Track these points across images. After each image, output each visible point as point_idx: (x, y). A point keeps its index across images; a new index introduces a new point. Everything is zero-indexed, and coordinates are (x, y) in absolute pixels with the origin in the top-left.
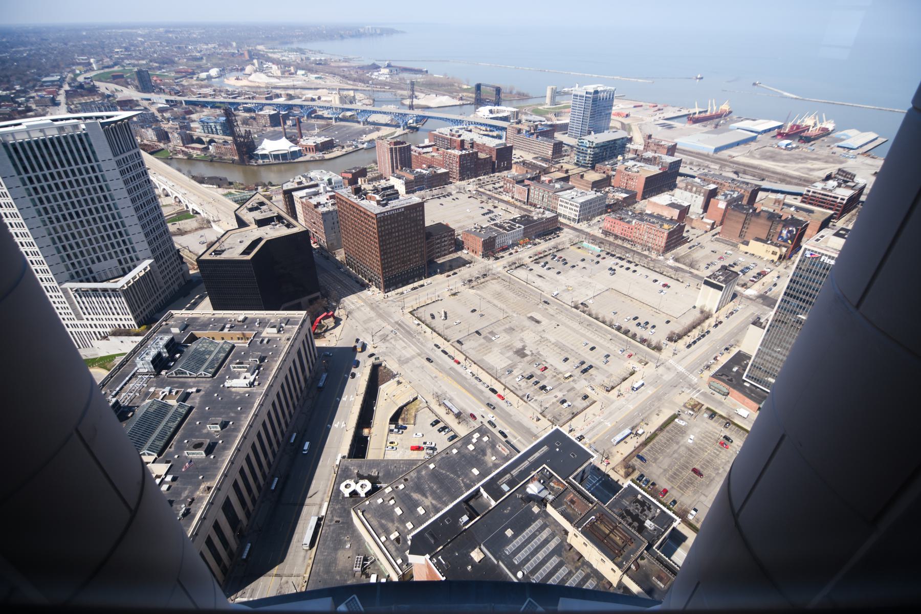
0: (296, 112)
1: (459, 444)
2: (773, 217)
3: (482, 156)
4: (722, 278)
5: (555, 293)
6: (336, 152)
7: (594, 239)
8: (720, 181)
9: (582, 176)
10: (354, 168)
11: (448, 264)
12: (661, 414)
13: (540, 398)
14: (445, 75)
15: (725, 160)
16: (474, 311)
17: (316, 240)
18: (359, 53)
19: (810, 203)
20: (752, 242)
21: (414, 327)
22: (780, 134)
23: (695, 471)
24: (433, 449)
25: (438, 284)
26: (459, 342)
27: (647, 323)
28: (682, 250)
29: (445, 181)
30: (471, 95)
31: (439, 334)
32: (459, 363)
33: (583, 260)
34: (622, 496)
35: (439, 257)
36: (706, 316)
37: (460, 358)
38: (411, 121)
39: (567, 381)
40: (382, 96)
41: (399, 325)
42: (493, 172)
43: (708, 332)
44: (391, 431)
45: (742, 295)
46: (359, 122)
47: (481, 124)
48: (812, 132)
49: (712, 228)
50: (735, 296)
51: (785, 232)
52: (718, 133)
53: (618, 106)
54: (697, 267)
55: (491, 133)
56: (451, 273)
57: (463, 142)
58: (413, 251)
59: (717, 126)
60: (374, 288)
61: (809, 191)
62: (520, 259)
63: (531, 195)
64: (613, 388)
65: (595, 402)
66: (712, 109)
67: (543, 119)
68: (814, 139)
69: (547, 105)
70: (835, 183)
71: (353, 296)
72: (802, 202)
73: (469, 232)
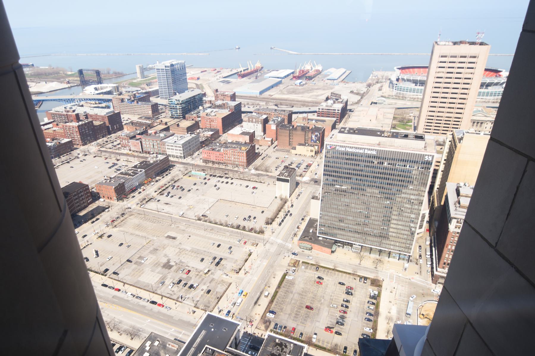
4: (286, 174)
5: (181, 213)
8: (268, 112)
9: (178, 125)
12: (276, 277)
13: (190, 296)
14: (50, 66)
15: (268, 99)
16: (121, 244)
22: (294, 77)
23: (308, 307)
26: (115, 273)
27: (250, 217)
28: (258, 162)
30: (76, 79)
32: (119, 290)
33: (195, 184)
34: (266, 346)
35: (80, 210)
36: (285, 201)
37: (119, 285)
39: (207, 275)
42: (110, 134)
45: (301, 182)
47: (90, 100)
48: (311, 73)
49: (272, 143)
50: (297, 184)
51: (313, 137)
52: (259, 82)
53: (190, 73)
54: (270, 171)
55: (100, 105)
56: (94, 219)
59: (256, 78)
62: (147, 195)
63: (144, 145)
64: (240, 269)
65: (231, 284)
66: (251, 67)
67: (139, 89)
68: (314, 77)
69: (139, 79)
70: (332, 102)
73: (101, 184)
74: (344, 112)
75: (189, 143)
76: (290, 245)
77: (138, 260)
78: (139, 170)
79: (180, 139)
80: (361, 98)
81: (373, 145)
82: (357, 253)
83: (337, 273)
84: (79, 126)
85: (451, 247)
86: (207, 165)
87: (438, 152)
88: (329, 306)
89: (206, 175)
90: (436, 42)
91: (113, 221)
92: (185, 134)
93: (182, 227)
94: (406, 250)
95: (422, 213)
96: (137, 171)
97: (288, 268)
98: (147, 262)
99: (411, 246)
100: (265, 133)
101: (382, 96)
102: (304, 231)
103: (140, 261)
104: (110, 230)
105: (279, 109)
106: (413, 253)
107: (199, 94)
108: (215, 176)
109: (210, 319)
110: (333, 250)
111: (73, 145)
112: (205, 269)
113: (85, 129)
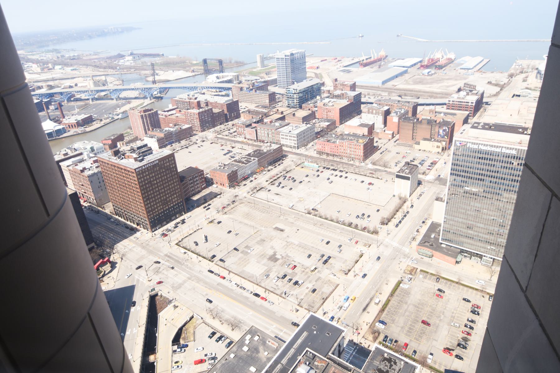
0: (57, 98)
1: (235, 349)
2: (430, 122)
4: (407, 171)
5: (291, 205)
6: (96, 125)
8: (390, 103)
9: (294, 115)
10: (113, 135)
11: (203, 199)
12: (389, 283)
16: (230, 232)
17: (85, 199)
18: (106, 47)
19: (452, 109)
21: (182, 256)
22: (422, 66)
23: (424, 322)
24: (214, 358)
25: (196, 217)
27: (363, 215)
28: (376, 156)
29: (190, 134)
31: (204, 258)
33: (307, 176)
38: (156, 93)
39: (314, 273)
40: (129, 77)
41: (169, 257)
42: (227, 121)
43: (408, 212)
44: (175, 351)
45: (424, 180)
46: (112, 99)
47: (211, 88)
48: (442, 62)
49: (393, 137)
51: (441, 131)
53: (310, 62)
54: (389, 166)
55: (220, 93)
58: (171, 194)
59: (380, 67)
60: (142, 230)
64: (349, 271)
65: (338, 285)
66: (374, 56)
67: (258, 78)
68: (444, 66)
69: (259, 68)
71: (126, 240)
74: (479, 105)
75: (304, 133)
76: (406, 250)
77: (244, 249)
78: (252, 158)
79: (294, 128)
80: (501, 90)
81: (514, 143)
82: (487, 266)
83: (461, 287)
84: (199, 113)
86: (321, 157)
88: (449, 324)
89: (319, 167)
91: (224, 208)
92: (300, 124)
93: (291, 220)
96: (250, 159)
97: (404, 275)
98: (253, 253)
101: (527, 88)
102: (425, 236)
103: (247, 250)
104: (220, 217)
105: (403, 100)
108: (329, 169)
109: (313, 320)
110: (458, 260)
111: (192, 131)
112: (312, 266)
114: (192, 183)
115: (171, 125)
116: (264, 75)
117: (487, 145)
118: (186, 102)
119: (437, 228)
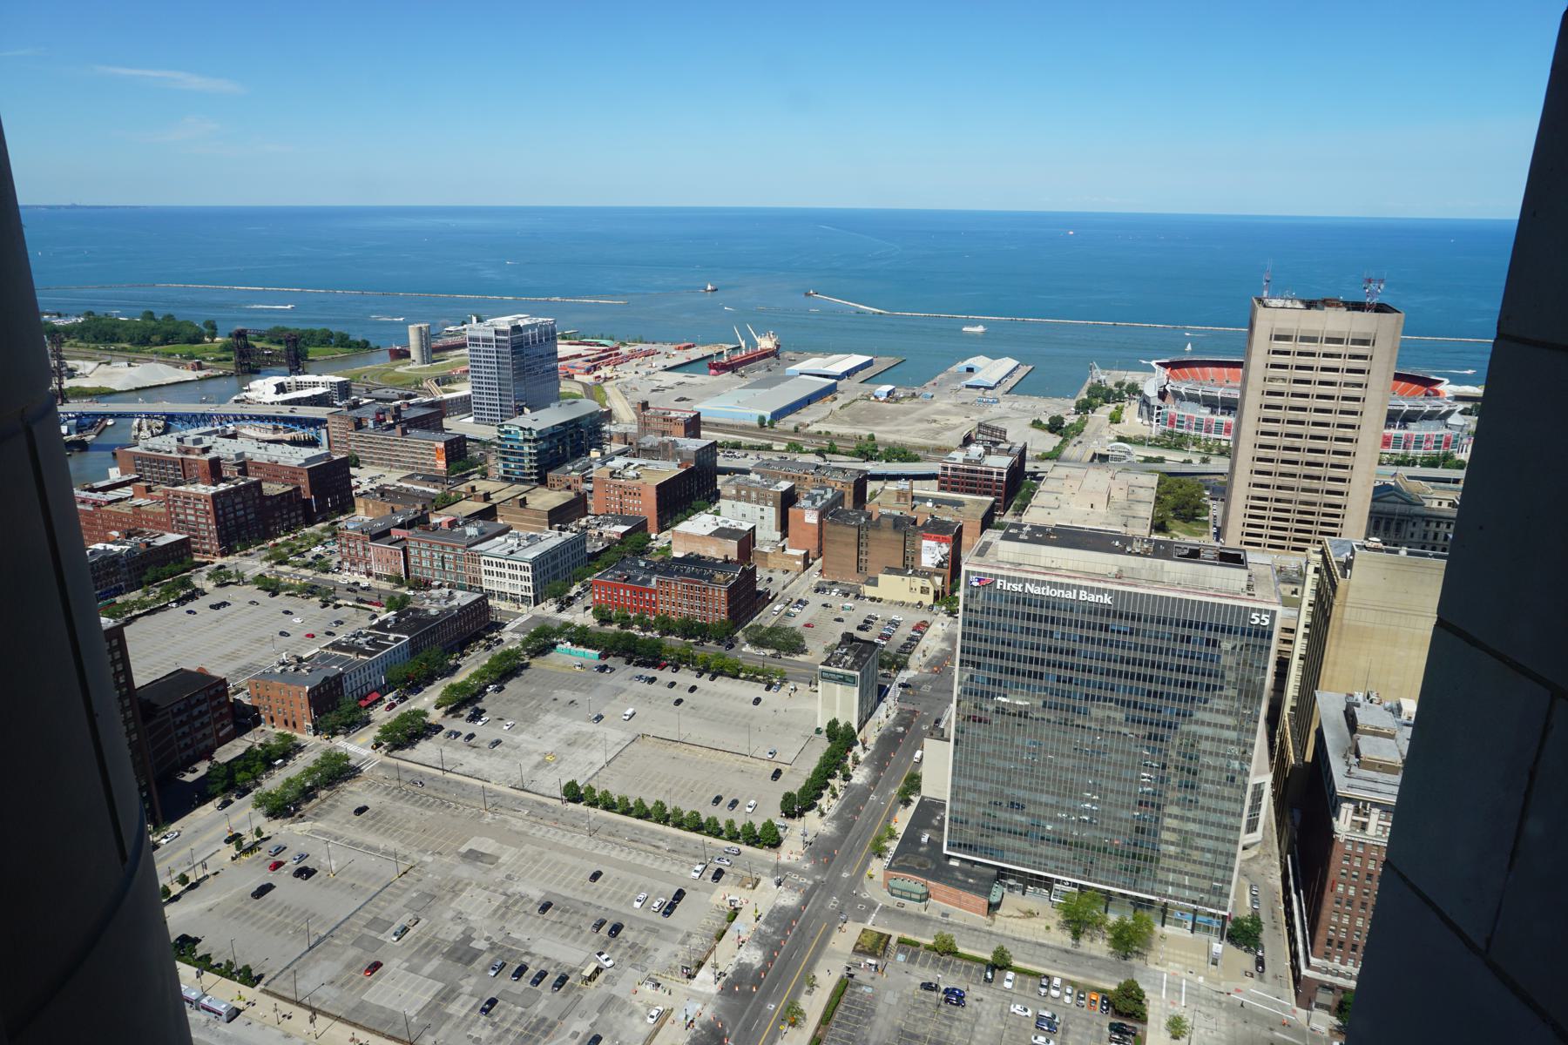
2: (899, 523)
3: (272, 489)
7: (581, 637)
8: (794, 472)
9: (523, 502)
20: (882, 578)
39: (593, 984)
49: (807, 565)
57: (215, 464)
61: (945, 468)
64: (700, 965)
72: (941, 489)
75: (554, 557)
77: (365, 931)
78: (392, 637)
79: (525, 543)
81: (1104, 577)
85: (1346, 890)
87: (1286, 602)
90: (1260, 300)
92: (542, 530)
94: (1214, 899)
95: (1253, 780)
96: (385, 638)
97: (855, 959)
99: (1226, 887)
100: (785, 535)
103: (373, 933)
106: (1234, 907)
107: (591, 415)
110: (994, 900)
111: (190, 553)
113: (234, 505)
114: (183, 723)
115: (115, 534)
116: (434, 387)
117: (1043, 583)
118: (174, 462)
119: (935, 815)
